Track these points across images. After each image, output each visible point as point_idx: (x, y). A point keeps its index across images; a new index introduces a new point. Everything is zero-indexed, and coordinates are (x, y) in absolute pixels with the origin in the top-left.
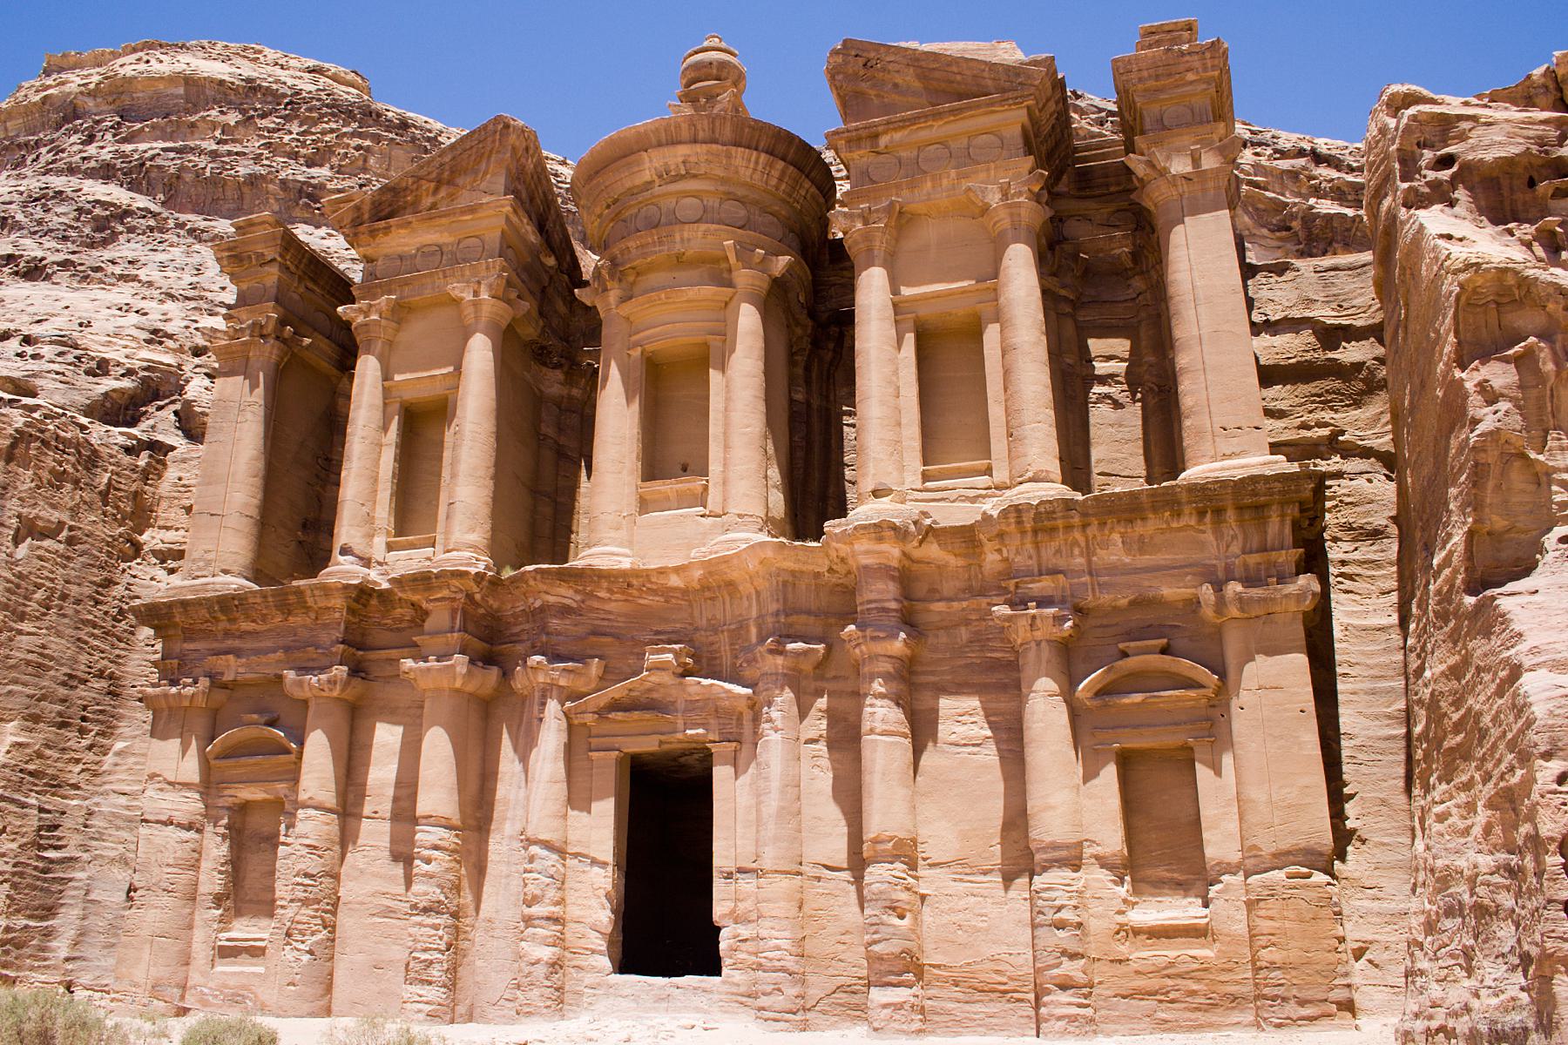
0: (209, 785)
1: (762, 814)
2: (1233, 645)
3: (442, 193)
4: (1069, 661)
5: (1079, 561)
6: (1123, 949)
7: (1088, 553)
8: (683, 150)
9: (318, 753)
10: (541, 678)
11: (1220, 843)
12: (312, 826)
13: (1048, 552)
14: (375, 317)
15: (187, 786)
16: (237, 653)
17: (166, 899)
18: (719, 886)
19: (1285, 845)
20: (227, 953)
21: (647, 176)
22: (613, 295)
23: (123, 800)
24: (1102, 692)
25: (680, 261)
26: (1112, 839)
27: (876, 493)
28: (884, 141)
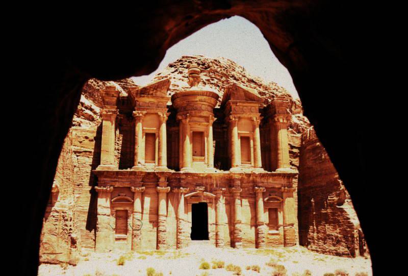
0: (112, 207)
1: (217, 215)
2: (284, 195)
3: (155, 91)
4: (264, 195)
5: (266, 181)
6: (269, 236)
7: (267, 180)
8: (205, 97)
9: (138, 202)
10: (181, 191)
11: (281, 222)
12: (138, 216)
13: (262, 179)
14: (141, 115)
15: (108, 208)
16: (118, 181)
17: (106, 230)
18: (209, 227)
19: (290, 223)
20: (117, 239)
21: (197, 100)
22: (188, 120)
23: (81, 208)
24: (268, 200)
25: (201, 117)
26: (267, 221)
27: (236, 166)
28: (238, 104)
